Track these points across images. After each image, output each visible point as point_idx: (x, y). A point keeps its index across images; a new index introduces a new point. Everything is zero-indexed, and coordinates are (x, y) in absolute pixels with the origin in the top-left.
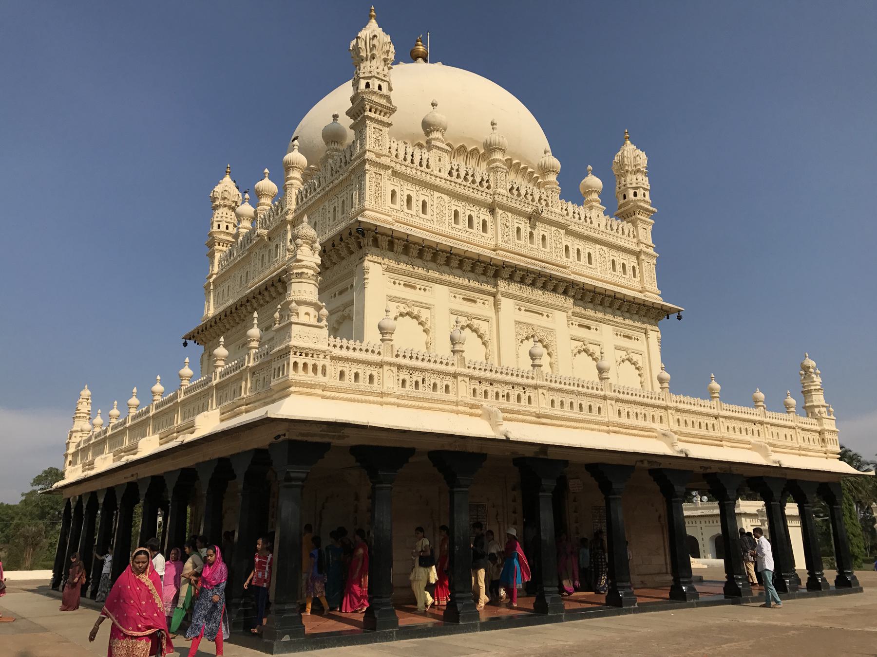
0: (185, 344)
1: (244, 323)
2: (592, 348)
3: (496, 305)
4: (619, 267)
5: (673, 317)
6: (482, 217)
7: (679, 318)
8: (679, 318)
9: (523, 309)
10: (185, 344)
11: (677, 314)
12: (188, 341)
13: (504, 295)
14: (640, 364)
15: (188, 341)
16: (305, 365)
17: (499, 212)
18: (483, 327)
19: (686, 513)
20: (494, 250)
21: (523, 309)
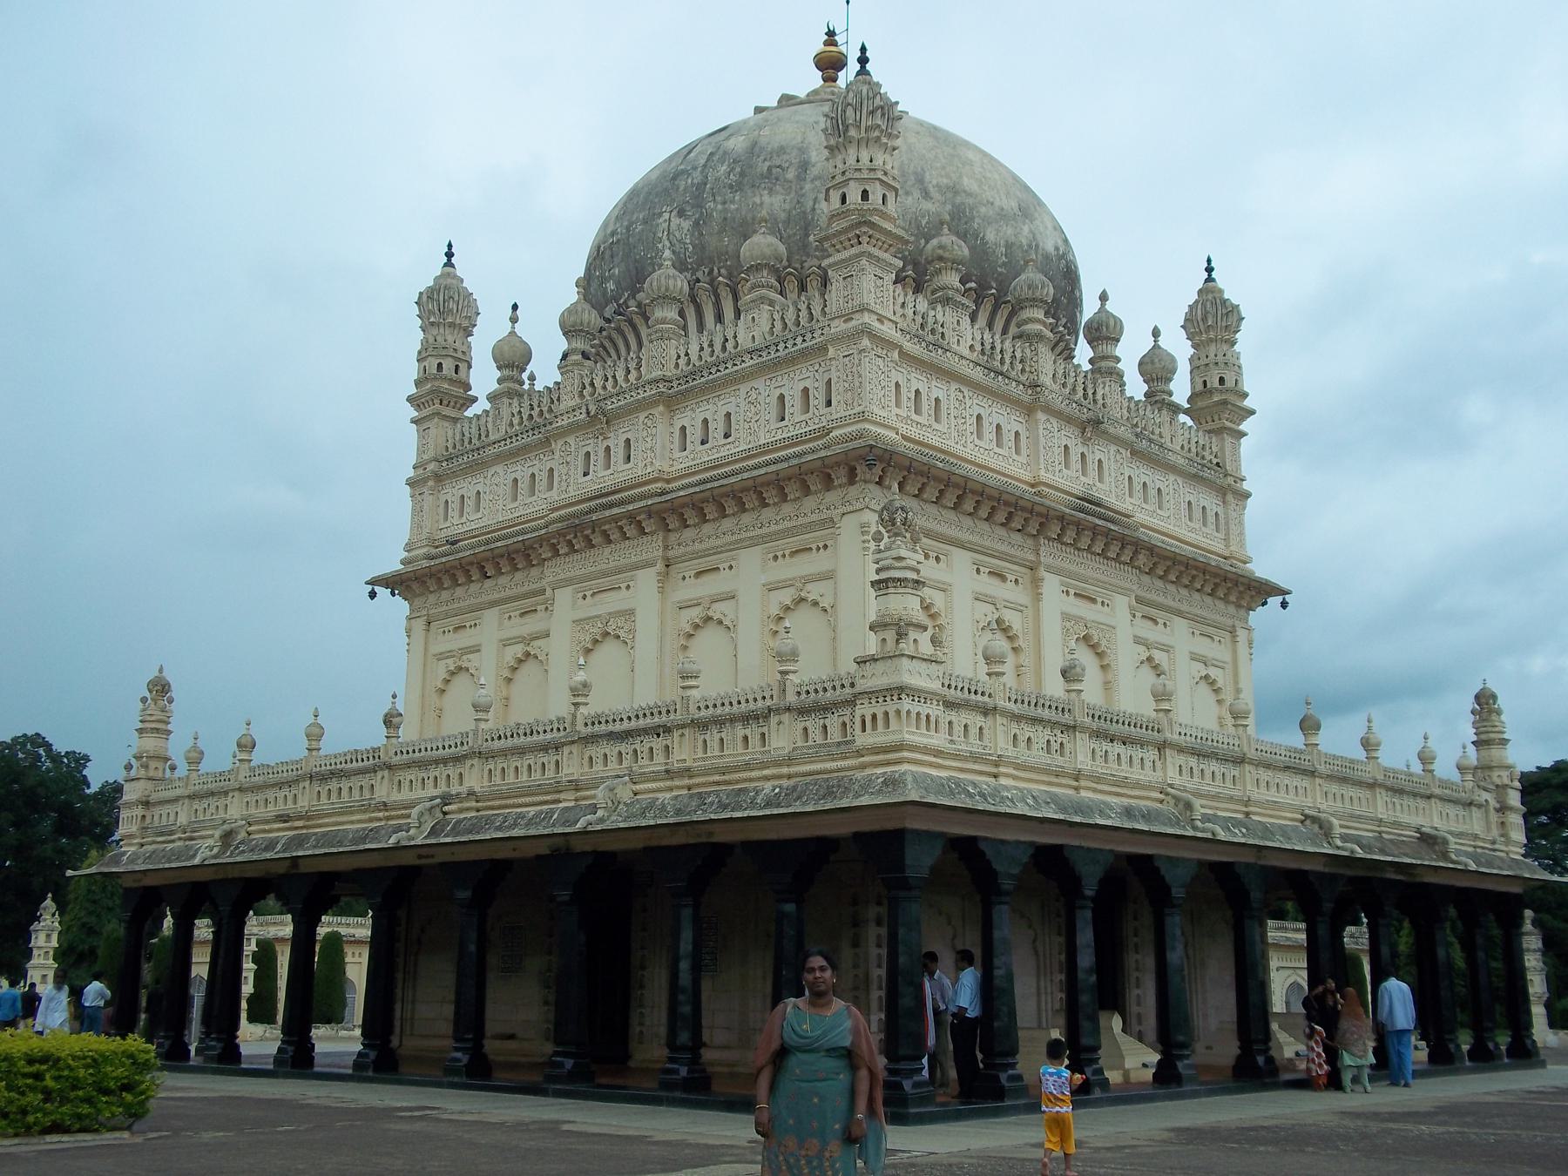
0: (373, 595)
1: (534, 572)
2: (1159, 656)
3: (1036, 583)
4: (1197, 514)
5: (1275, 601)
6: (1016, 427)
7: (1284, 605)
8: (1284, 605)
9: (1072, 592)
10: (373, 595)
11: (1280, 598)
12: (377, 589)
13: (1049, 569)
14: (1220, 683)
15: (377, 589)
16: (918, 714)
17: (1041, 416)
18: (1012, 618)
19: (1304, 936)
20: (1033, 486)
21: (1072, 592)
